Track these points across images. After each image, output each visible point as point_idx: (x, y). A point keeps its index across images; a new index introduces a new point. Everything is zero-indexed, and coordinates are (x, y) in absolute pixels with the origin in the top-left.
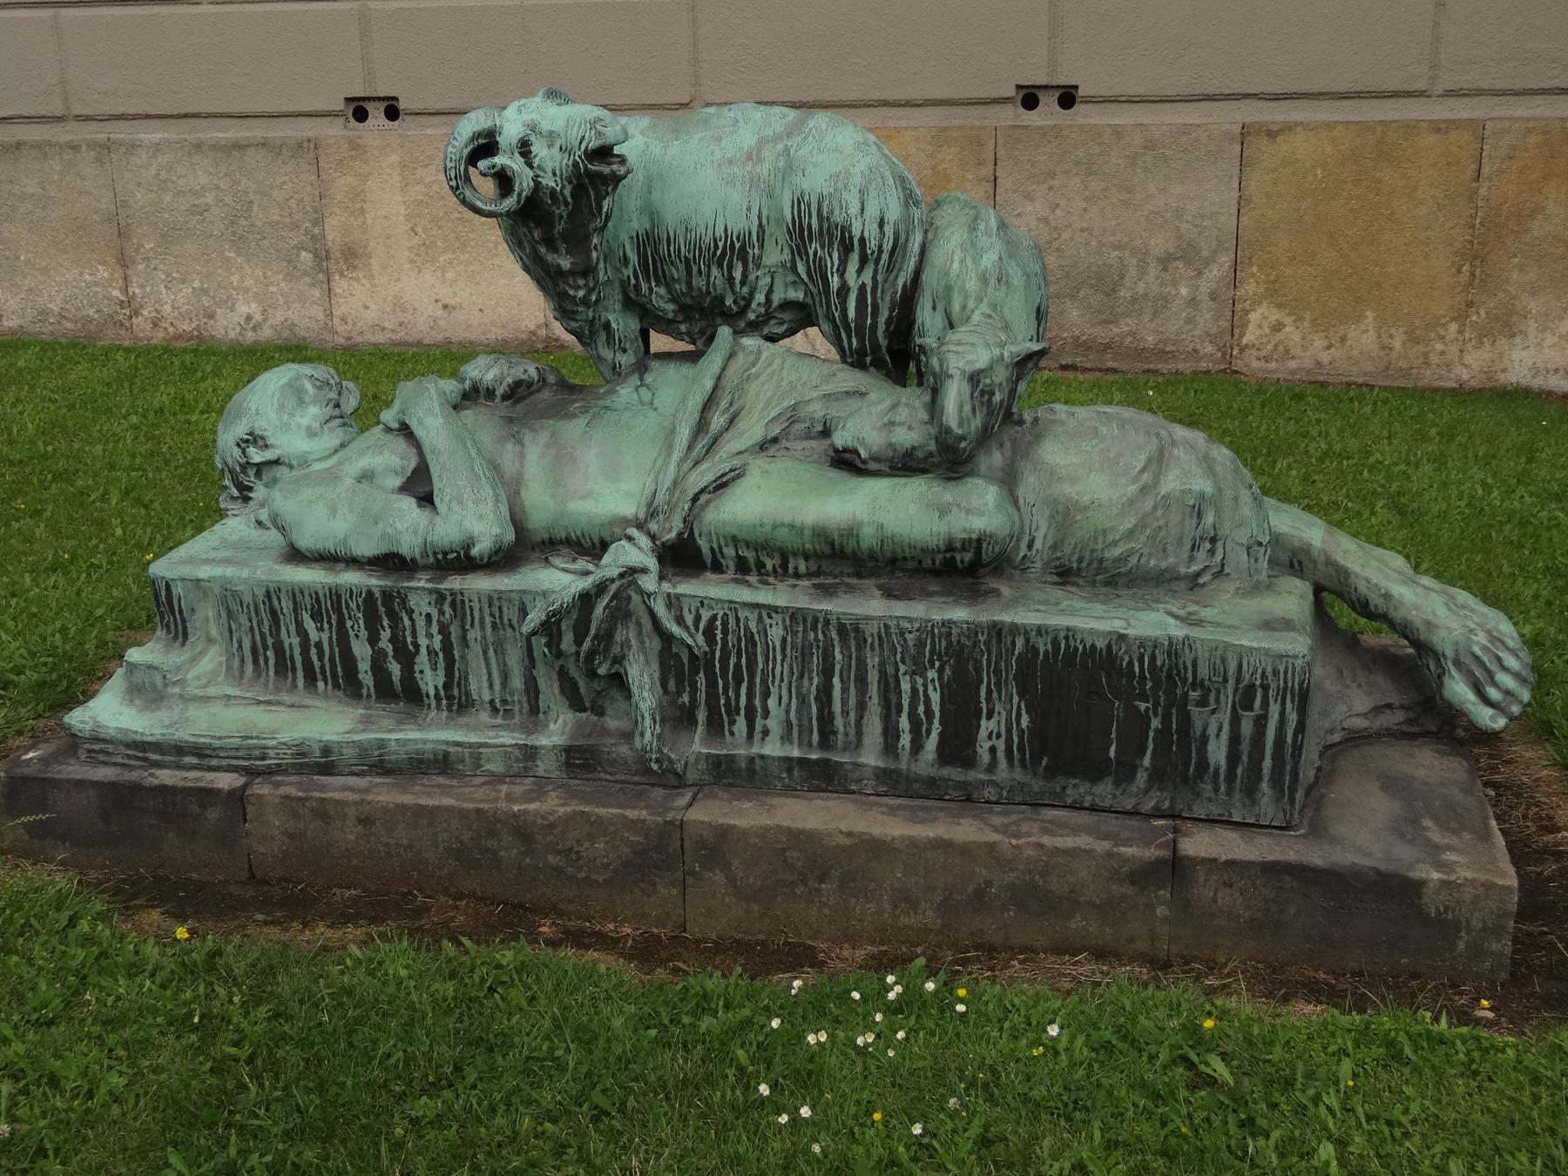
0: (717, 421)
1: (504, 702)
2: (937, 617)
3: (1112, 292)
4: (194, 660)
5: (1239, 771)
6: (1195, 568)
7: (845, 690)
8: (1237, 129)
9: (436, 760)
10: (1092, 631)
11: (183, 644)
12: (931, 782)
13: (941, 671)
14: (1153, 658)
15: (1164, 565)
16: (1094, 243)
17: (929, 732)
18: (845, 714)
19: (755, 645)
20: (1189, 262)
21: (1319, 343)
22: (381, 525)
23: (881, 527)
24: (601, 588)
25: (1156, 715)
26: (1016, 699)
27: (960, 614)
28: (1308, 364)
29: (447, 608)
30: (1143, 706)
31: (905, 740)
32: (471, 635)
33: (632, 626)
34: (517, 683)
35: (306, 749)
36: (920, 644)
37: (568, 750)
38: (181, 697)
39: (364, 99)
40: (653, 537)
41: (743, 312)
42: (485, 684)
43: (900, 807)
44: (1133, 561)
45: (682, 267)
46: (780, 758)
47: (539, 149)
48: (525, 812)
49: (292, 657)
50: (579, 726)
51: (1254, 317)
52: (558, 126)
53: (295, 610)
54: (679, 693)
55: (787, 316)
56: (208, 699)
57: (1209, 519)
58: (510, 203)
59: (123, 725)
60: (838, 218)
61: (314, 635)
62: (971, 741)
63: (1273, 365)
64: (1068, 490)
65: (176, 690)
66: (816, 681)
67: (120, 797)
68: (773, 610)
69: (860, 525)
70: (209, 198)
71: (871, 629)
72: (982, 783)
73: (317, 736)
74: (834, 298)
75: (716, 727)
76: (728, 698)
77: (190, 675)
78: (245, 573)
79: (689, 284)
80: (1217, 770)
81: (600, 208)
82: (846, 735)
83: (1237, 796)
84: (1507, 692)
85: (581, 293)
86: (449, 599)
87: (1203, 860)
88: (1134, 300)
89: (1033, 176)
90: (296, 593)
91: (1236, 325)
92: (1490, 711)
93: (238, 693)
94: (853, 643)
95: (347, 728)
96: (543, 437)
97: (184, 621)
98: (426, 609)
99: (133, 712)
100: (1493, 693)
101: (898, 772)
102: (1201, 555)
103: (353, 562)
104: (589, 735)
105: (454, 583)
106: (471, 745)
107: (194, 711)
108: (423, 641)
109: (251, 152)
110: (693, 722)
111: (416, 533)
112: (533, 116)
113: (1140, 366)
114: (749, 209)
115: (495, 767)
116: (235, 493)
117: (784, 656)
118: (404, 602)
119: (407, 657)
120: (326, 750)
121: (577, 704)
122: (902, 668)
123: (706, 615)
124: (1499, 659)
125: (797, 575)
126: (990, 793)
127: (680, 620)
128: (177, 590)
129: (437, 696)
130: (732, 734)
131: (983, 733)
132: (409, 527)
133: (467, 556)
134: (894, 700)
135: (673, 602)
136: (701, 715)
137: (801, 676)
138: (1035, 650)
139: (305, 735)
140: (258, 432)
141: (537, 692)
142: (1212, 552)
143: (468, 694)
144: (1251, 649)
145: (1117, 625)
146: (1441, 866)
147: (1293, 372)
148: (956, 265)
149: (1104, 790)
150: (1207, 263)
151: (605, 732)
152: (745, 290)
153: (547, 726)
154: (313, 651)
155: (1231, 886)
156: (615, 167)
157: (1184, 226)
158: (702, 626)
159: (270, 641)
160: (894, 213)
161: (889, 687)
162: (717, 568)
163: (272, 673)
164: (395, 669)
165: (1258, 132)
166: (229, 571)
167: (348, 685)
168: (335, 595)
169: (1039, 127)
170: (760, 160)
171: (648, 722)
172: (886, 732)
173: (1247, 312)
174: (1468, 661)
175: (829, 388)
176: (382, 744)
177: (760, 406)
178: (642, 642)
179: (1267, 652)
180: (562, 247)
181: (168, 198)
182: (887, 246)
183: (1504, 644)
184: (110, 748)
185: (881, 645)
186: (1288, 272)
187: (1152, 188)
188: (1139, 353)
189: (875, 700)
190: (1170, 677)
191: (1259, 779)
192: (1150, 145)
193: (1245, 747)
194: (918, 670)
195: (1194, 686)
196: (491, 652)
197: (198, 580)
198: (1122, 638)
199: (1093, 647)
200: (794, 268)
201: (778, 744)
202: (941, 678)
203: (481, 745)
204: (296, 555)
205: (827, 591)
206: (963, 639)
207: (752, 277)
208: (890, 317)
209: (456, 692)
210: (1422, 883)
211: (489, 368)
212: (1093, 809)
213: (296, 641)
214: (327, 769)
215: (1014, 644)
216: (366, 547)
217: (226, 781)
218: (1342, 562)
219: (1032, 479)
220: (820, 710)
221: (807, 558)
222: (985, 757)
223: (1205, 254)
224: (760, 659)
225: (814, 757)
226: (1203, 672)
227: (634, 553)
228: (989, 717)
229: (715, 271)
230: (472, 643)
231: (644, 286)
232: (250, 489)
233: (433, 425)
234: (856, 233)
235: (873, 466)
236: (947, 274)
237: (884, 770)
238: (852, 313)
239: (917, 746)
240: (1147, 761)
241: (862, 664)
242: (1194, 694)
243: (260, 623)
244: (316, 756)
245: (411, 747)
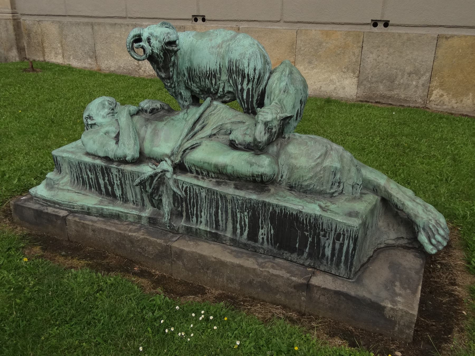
0: (198, 127)
1: (136, 201)
2: (247, 197)
3: (393, 82)
4: (62, 178)
5: (334, 259)
6: (332, 191)
7: (222, 214)
8: (436, 36)
10: (292, 209)
11: (60, 173)
12: (245, 245)
13: (248, 213)
15: (322, 189)
16: (389, 67)
17: (245, 230)
18: (222, 221)
19: (198, 197)
20: (417, 75)
21: (454, 101)
23: (233, 167)
24: (156, 174)
25: (310, 237)
26: (270, 225)
27: (254, 197)
28: (450, 107)
30: (307, 234)
31: (239, 231)
33: (165, 187)
34: (139, 197)
36: (242, 204)
37: (149, 218)
38: (58, 188)
39: (197, 16)
40: (172, 161)
41: (217, 93)
42: (131, 196)
43: (235, 251)
44: (312, 186)
45: (198, 78)
46: (204, 230)
47: (153, 41)
48: (132, 235)
50: (154, 211)
51: (435, 92)
52: (158, 34)
54: (178, 207)
55: (230, 95)
57: (338, 176)
59: (42, 194)
60: (241, 67)
61: (90, 176)
62: (257, 235)
63: (439, 107)
64: (294, 161)
65: (57, 186)
66: (214, 210)
67: (39, 213)
68: (202, 188)
69: (227, 166)
71: (229, 197)
72: (259, 247)
73: (86, 204)
75: (188, 219)
76: (191, 211)
77: (61, 182)
78: (74, 157)
79: (200, 84)
80: (328, 257)
81: (171, 60)
82: (223, 227)
83: (334, 266)
84: (438, 242)
85: (169, 84)
87: (316, 286)
88: (399, 85)
89: (373, 47)
90: (85, 164)
91: (429, 94)
92: (431, 247)
93: (71, 189)
94: (224, 201)
95: (96, 203)
96: (153, 126)
98: (116, 173)
99: (46, 190)
100: (433, 241)
102: (335, 187)
103: (99, 157)
104: (155, 215)
105: (122, 167)
106: (125, 213)
107: (60, 193)
108: (115, 182)
110: (182, 216)
112: (152, 31)
113: (398, 104)
114: (216, 63)
115: (131, 219)
117: (206, 201)
118: (110, 170)
119: (112, 185)
120: (88, 209)
121: (153, 205)
122: (238, 210)
123: (185, 186)
124: (438, 230)
126: (261, 251)
127: (178, 187)
128: (59, 159)
129: (120, 197)
130: (192, 221)
131: (260, 233)
132: (112, 149)
133: (125, 159)
134: (235, 219)
135: (176, 181)
136: (184, 214)
137: (210, 208)
138: (275, 212)
139: (84, 204)
140: (91, 115)
141: (144, 201)
142: (339, 186)
143: (127, 198)
144: (340, 222)
145: (300, 208)
146: (394, 302)
147: (445, 109)
148: (274, 85)
149: (294, 256)
150: (422, 75)
152: (216, 87)
154: (90, 180)
155: (324, 296)
156: (173, 48)
157: (417, 64)
158: (184, 189)
159: (80, 176)
160: (259, 67)
164: (110, 188)
165: (443, 37)
168: (94, 166)
169: (377, 33)
170: (222, 47)
171: (166, 215)
172: (233, 228)
173: (433, 91)
174: (427, 229)
175: (233, 120)
176: (102, 209)
177: (212, 124)
178: (167, 192)
179: (345, 224)
180: (163, 70)
182: (257, 77)
183: (440, 225)
184: (39, 200)
185: (232, 202)
186: (447, 80)
187: (408, 52)
188: (399, 100)
189: (230, 218)
190: (314, 226)
191: (341, 262)
192: (409, 39)
193: (336, 252)
194: (242, 212)
195: (322, 230)
197: (63, 157)
198: (301, 212)
199: (292, 213)
200: (229, 81)
201: (204, 226)
202: (248, 215)
203: (128, 213)
204: (88, 154)
205: (218, 183)
206: (255, 205)
207: (218, 83)
208: (257, 99)
210: (384, 308)
211: (147, 103)
212: (291, 261)
213: (86, 177)
214: (89, 214)
215: (269, 208)
216: (102, 154)
217: (63, 213)
218: (390, 191)
219: (283, 157)
220: (215, 218)
221: (214, 173)
223: (422, 72)
224: (199, 201)
225: (213, 231)
226: (325, 227)
227: (166, 166)
228: (262, 229)
229: (207, 81)
231: (189, 83)
234: (246, 72)
235: (239, 146)
236: (272, 87)
237: (232, 239)
238: (245, 97)
239: (242, 234)
240: (307, 250)
241: (226, 207)
242: (322, 233)
243: (78, 170)
245: (110, 211)
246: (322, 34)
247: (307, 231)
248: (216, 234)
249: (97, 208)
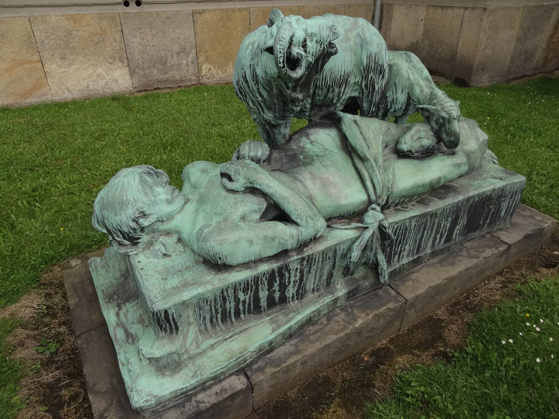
2: (456, 201)
3: (165, 64)
4: (185, 338)
7: (427, 233)
8: (191, 12)
11: (177, 333)
16: (157, 50)
20: (185, 53)
21: (220, 73)
22: (277, 241)
28: (219, 78)
34: (325, 277)
37: (348, 293)
38: (190, 358)
49: (230, 312)
50: (347, 282)
51: (203, 67)
53: (235, 292)
56: (204, 352)
59: (172, 390)
60: (380, 62)
63: (210, 80)
65: (186, 356)
77: (188, 346)
78: (210, 287)
88: (171, 66)
89: (134, 29)
91: (199, 70)
93: (215, 341)
97: (175, 323)
99: (169, 379)
103: (262, 260)
104: (353, 284)
105: (308, 252)
108: (292, 279)
111: (293, 238)
113: (176, 85)
120: (270, 343)
141: (332, 277)
147: (215, 81)
148: (411, 76)
150: (189, 53)
153: (336, 287)
157: (181, 42)
163: (220, 322)
165: (196, 13)
169: (133, 13)
170: (350, 40)
173: (202, 66)
187: (171, 31)
188: (176, 81)
192: (168, 18)
216: (274, 252)
223: (188, 50)
225: (416, 257)
236: (409, 79)
241: (434, 223)
244: (267, 348)
246: (68, 19)
248: (419, 258)
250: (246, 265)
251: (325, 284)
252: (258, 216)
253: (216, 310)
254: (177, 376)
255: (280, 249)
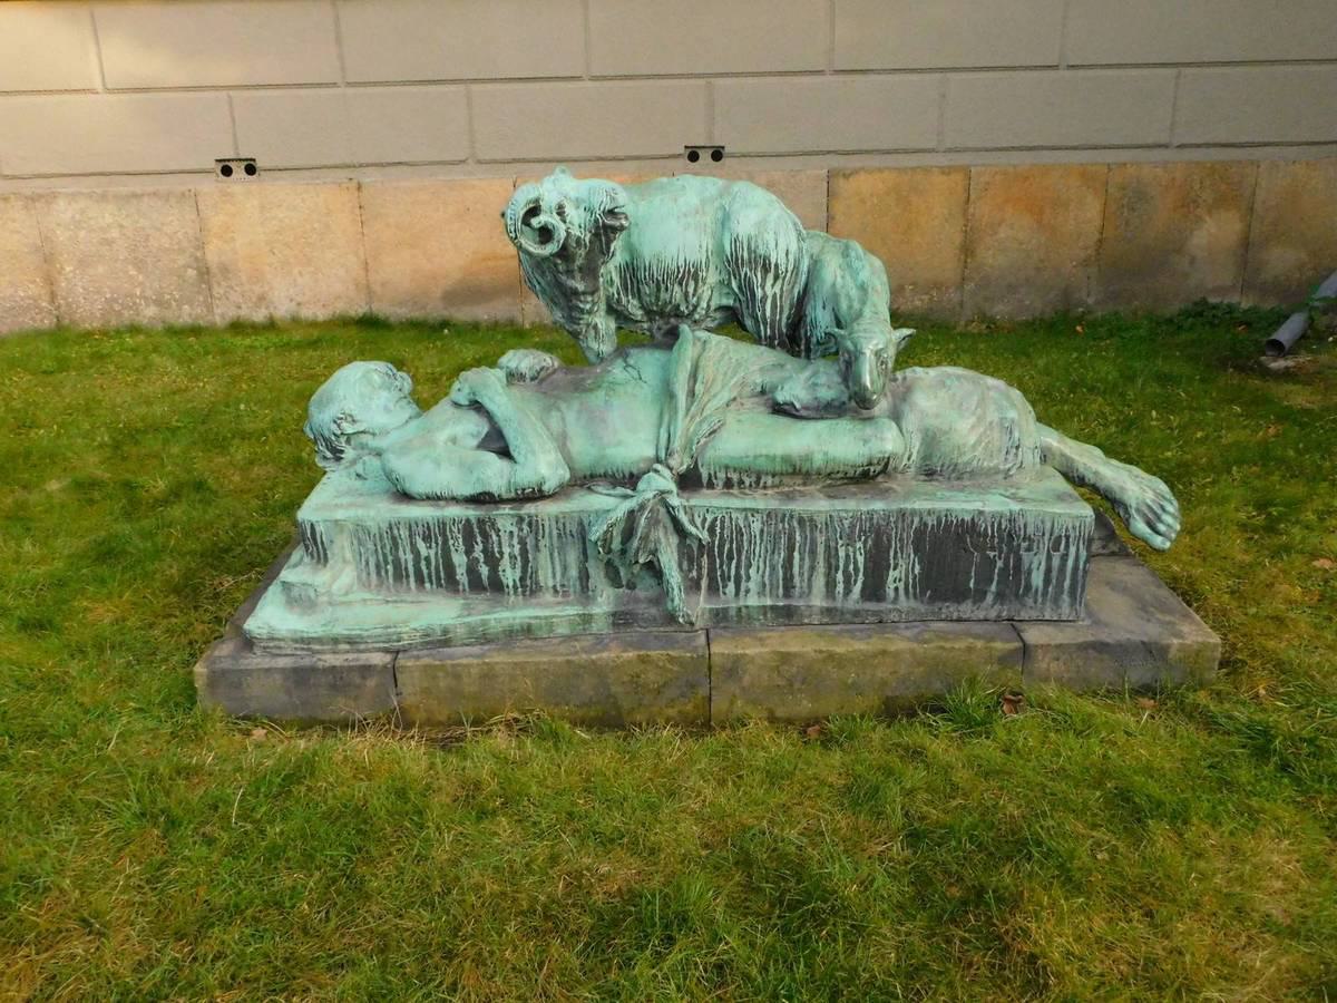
0: (699, 388)
1: (563, 586)
2: (864, 509)
4: (335, 578)
6: (1008, 466)
7: (802, 559)
9: (523, 630)
12: (856, 613)
13: (865, 542)
14: (1000, 524)
17: (856, 581)
18: (801, 574)
23: (826, 454)
24: (642, 507)
27: (878, 505)
29: (525, 527)
30: (992, 554)
31: (840, 588)
32: (542, 543)
34: (574, 572)
35: (430, 631)
36: (852, 526)
37: (614, 614)
38: (330, 604)
40: (671, 469)
42: (550, 575)
43: (842, 631)
45: (653, 286)
47: (569, 210)
48: (600, 659)
49: (406, 568)
50: (618, 597)
52: (583, 194)
53: (410, 536)
54: (690, 571)
56: (349, 603)
57: (1016, 435)
58: (551, 248)
59: (292, 627)
60: (761, 251)
61: (424, 551)
67: (301, 677)
70: (115, 233)
71: (820, 520)
74: (758, 304)
75: (713, 589)
76: (723, 571)
78: (372, 513)
79: (658, 298)
80: (1037, 590)
81: (609, 248)
83: (1048, 604)
84: (1169, 526)
85: (588, 307)
86: (527, 520)
96: (576, 405)
97: (325, 550)
98: (509, 528)
100: (1162, 528)
101: (836, 609)
102: (1011, 457)
103: (454, 500)
105: (529, 509)
106: (546, 618)
107: (341, 612)
108: (506, 550)
109: (146, 199)
110: (698, 587)
115: (563, 630)
116: (329, 455)
117: (762, 540)
118: (493, 525)
119: (493, 561)
120: (445, 631)
121: (615, 581)
122: (840, 542)
123: (710, 518)
125: (765, 487)
126: (894, 616)
127: (692, 522)
128: (320, 528)
129: (515, 587)
131: (890, 579)
132: (494, 474)
133: (540, 491)
134: (833, 561)
135: (689, 511)
136: (704, 583)
138: (926, 525)
141: (588, 577)
142: (1016, 455)
143: (537, 583)
144: (1060, 515)
145: (978, 506)
146: (1179, 635)
148: (839, 279)
149: (966, 609)
151: (637, 600)
154: (423, 565)
158: (707, 525)
159: (390, 558)
160: (793, 248)
161: (831, 554)
162: (711, 485)
163: (391, 580)
164: (484, 570)
166: (360, 512)
167: (449, 582)
168: (442, 525)
171: (676, 591)
172: (827, 584)
179: (1069, 515)
180: (578, 276)
181: (82, 234)
182: (790, 268)
184: (282, 644)
189: (822, 564)
190: (1010, 536)
193: (1054, 574)
194: (850, 542)
195: (1024, 539)
196: (556, 554)
197: (336, 521)
198: (981, 513)
200: (729, 285)
203: (553, 617)
204: (405, 496)
205: (789, 497)
206: (881, 522)
207: (700, 291)
209: (528, 582)
210: (1169, 646)
212: (959, 620)
213: (410, 557)
216: (468, 491)
217: (378, 659)
220: (785, 574)
221: (773, 476)
222: (891, 593)
224: (745, 544)
226: (1030, 530)
227: (663, 481)
228: (895, 569)
229: (677, 288)
230: (542, 548)
231: (624, 300)
232: (342, 452)
233: (501, 400)
234: (773, 261)
235: (804, 413)
238: (768, 313)
239: (848, 591)
240: (993, 587)
241: (814, 543)
244: (438, 635)
245: (505, 623)
247: (993, 549)
249: (468, 625)
250: (434, 499)
251: (578, 587)
252: (475, 442)
253: (385, 555)
254: (306, 618)
255: (479, 490)
